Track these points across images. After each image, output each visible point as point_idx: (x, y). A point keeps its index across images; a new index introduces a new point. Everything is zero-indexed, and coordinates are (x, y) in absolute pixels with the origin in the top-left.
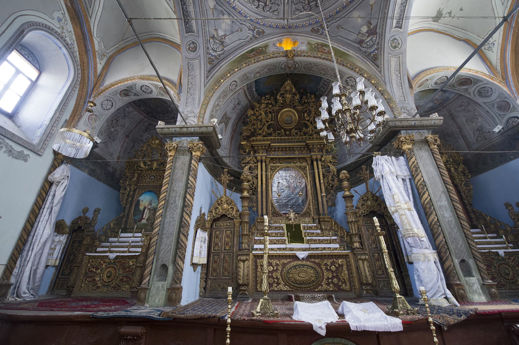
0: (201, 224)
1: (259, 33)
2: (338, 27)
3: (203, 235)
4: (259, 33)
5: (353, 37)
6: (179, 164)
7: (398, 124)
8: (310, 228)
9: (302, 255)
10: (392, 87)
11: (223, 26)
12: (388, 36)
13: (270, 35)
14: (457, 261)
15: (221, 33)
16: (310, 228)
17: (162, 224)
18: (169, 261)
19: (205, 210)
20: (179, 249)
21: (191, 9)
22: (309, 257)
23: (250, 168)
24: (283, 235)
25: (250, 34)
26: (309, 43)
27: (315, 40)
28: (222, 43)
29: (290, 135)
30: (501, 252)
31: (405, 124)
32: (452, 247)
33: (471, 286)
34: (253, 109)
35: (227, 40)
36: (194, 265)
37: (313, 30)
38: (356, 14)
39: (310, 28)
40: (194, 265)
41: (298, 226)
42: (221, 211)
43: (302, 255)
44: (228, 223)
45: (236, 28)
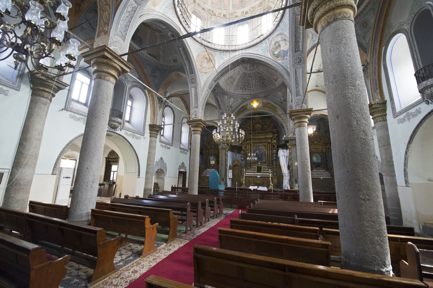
0: (230, 168)
1: (244, 99)
2: (274, 96)
3: (231, 171)
4: (244, 99)
5: (279, 100)
6: (223, 153)
7: (287, 139)
8: (265, 168)
9: (258, 176)
10: (290, 123)
11: (231, 101)
12: (288, 105)
13: (248, 99)
14: (294, 180)
15: (230, 104)
16: (265, 168)
17: (221, 169)
18: (224, 177)
19: (231, 164)
20: (226, 175)
21: (221, 103)
22: (261, 177)
23: (245, 147)
24: (255, 170)
25: (241, 100)
26: (263, 103)
27: (265, 101)
28: (231, 107)
29: (259, 133)
30: (322, 178)
31: (290, 139)
32: (294, 176)
33: (295, 186)
34: (244, 125)
35: (233, 105)
36: (229, 179)
37: (264, 96)
38: (279, 93)
39: (263, 96)
40: (229, 179)
41: (261, 167)
42: (235, 164)
43: (258, 176)
44: (237, 167)
45: (235, 100)
